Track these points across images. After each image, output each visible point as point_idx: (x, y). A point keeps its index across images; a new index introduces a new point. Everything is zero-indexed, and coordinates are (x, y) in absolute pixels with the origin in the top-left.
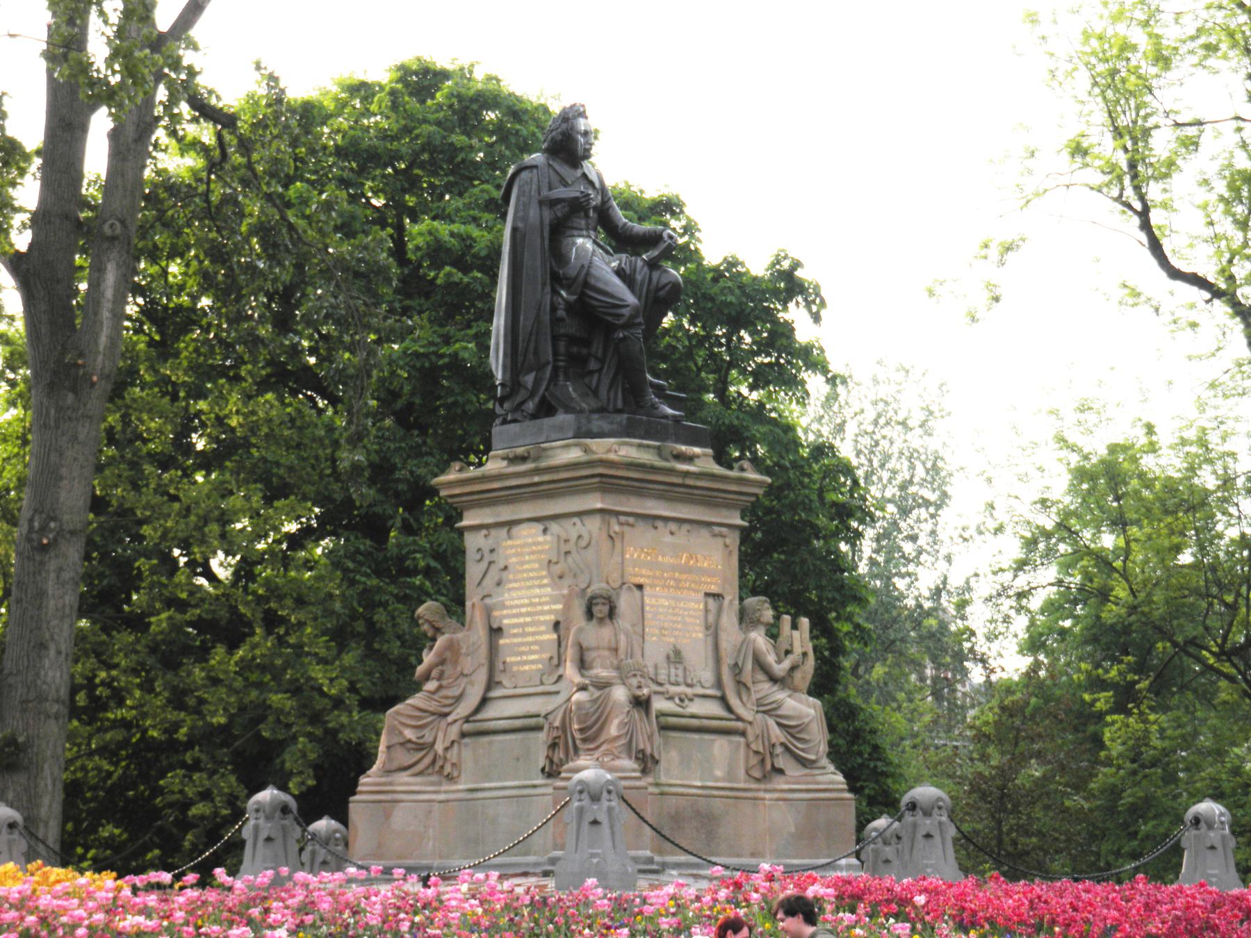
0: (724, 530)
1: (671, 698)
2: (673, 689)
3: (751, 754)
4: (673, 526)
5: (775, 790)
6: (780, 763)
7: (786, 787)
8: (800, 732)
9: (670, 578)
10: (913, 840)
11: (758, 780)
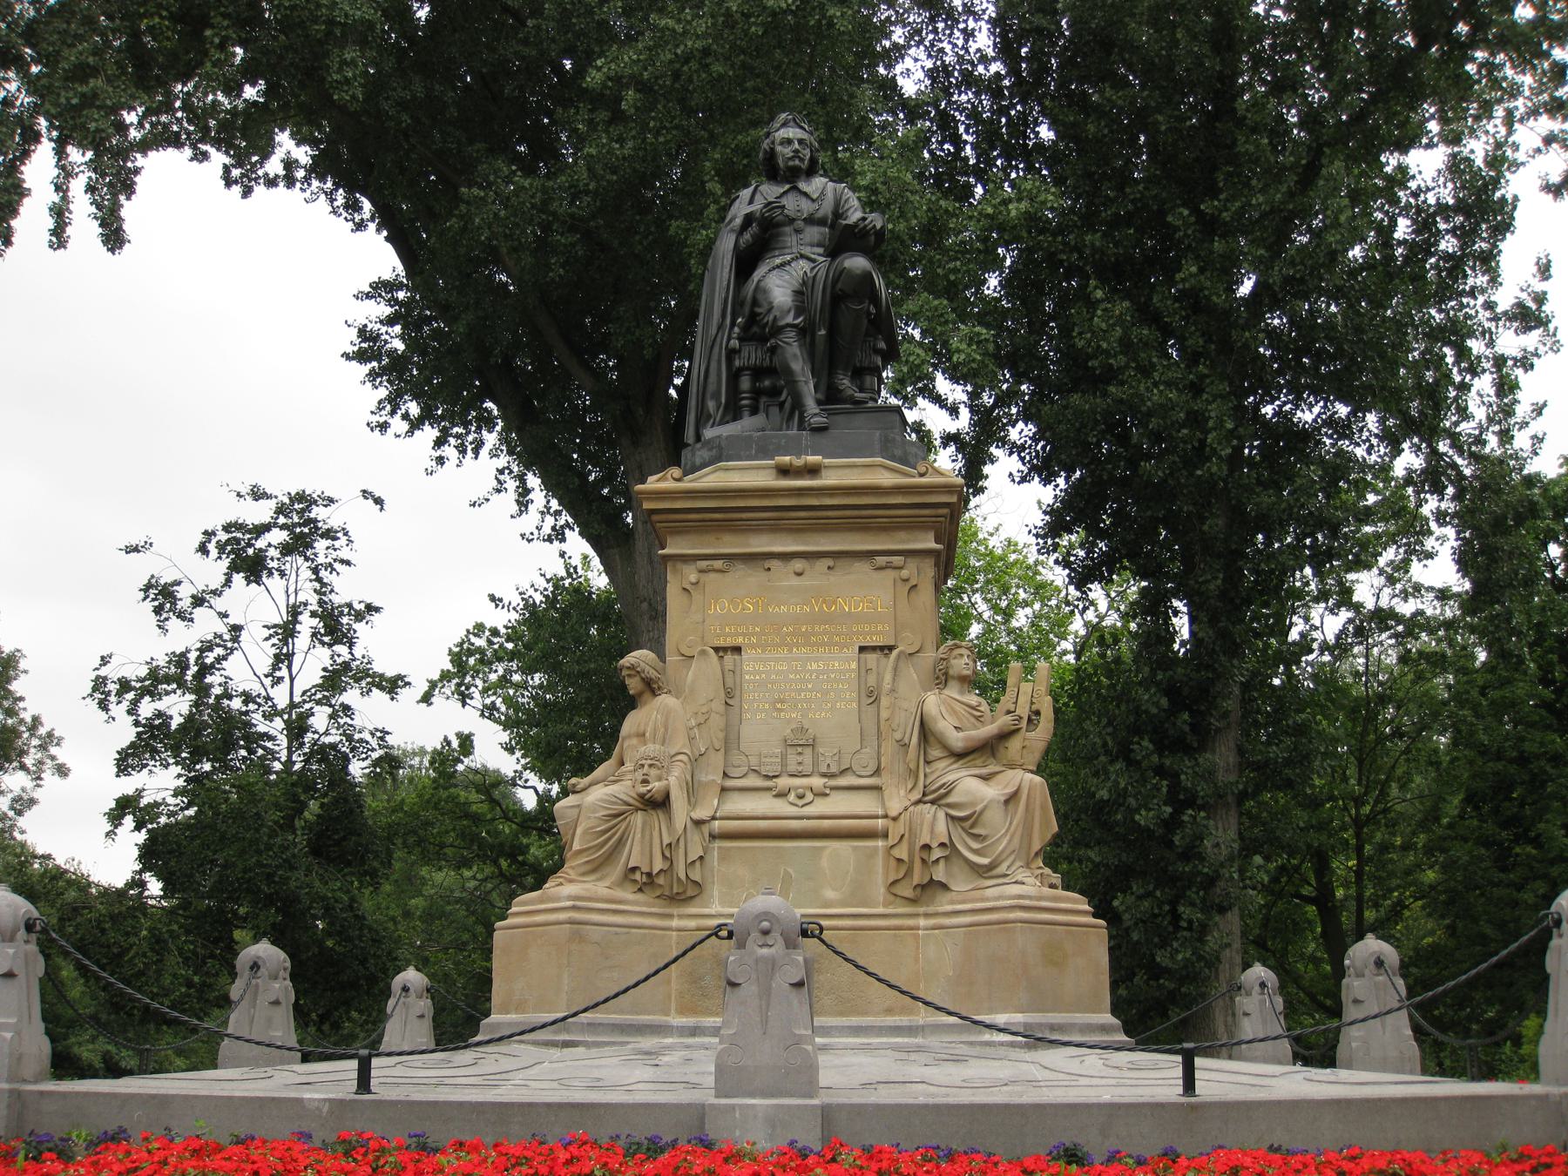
1: (782, 795)
2: (783, 782)
3: (893, 863)
4: (798, 565)
5: (936, 914)
6: (939, 874)
7: (949, 908)
8: (972, 826)
9: (792, 634)
10: (766, 993)
11: (913, 901)
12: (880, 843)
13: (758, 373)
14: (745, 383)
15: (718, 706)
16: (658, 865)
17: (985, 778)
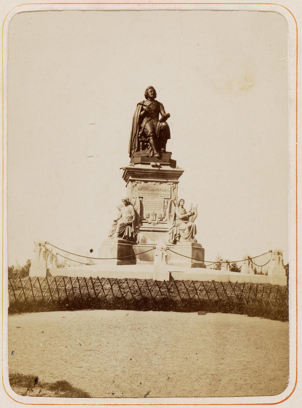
0: (172, 183)
12: (167, 233)
13: (144, 142)
14: (141, 143)
15: (139, 207)
16: (130, 235)
17: (186, 223)
